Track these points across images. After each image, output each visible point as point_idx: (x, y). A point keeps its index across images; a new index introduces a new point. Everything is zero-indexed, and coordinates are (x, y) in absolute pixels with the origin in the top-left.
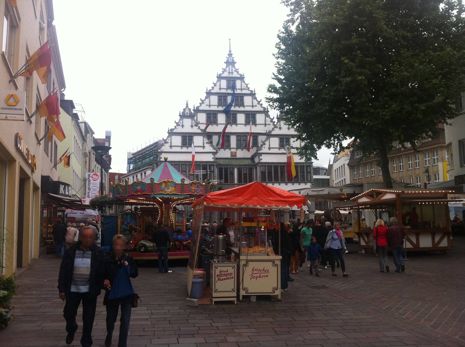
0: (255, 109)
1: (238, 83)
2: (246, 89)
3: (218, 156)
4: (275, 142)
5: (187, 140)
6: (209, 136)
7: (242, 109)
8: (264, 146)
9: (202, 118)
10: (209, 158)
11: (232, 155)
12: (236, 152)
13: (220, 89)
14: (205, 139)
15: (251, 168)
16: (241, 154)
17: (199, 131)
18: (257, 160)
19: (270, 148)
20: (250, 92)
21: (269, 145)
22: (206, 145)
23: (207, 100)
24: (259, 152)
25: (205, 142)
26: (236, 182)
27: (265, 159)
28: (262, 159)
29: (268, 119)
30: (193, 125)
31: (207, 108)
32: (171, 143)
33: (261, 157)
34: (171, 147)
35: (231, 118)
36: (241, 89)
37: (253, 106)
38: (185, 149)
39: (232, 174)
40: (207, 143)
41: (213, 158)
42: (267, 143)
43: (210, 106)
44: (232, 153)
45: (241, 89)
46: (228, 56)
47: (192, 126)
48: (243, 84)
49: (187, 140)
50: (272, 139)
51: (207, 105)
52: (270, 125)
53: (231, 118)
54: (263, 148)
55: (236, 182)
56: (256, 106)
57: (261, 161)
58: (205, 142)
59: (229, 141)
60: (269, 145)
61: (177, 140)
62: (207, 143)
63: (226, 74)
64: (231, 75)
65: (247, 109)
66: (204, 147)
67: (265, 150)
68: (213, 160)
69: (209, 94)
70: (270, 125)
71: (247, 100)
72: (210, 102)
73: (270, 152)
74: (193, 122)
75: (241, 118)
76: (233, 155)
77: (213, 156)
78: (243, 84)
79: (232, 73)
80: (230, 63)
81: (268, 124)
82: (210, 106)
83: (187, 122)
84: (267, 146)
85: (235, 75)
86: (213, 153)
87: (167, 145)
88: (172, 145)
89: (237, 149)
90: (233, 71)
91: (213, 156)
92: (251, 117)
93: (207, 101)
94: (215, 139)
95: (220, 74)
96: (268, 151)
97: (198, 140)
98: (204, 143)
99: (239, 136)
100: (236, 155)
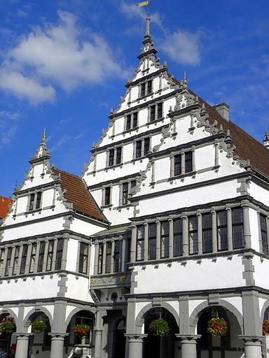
2: (168, 88)
4: (164, 166)
8: (143, 182)
14: (57, 192)
19: (152, 184)
21: (153, 176)
24: (134, 196)
25: (57, 197)
26: (123, 271)
31: (110, 142)
42: (149, 174)
60: (153, 176)
62: (58, 199)
64: (146, 74)
67: (144, 189)
72: (114, 130)
77: (64, 222)
79: (148, 69)
84: (148, 181)
90: (150, 67)
98: (54, 200)
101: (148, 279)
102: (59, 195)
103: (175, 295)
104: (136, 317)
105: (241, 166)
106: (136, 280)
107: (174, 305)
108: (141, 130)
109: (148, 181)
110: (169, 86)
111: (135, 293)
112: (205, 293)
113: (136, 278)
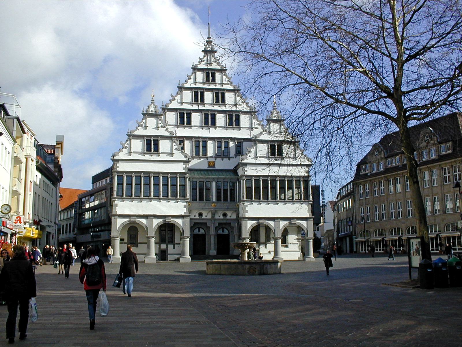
0: (239, 108)
1: (218, 75)
2: (228, 84)
3: (191, 165)
4: (263, 149)
5: (152, 145)
6: (181, 140)
7: (222, 108)
8: (249, 154)
9: (171, 118)
10: (180, 168)
11: (209, 166)
12: (214, 163)
13: (195, 83)
14: (174, 144)
15: (233, 183)
16: (220, 164)
17: (168, 134)
18: (240, 172)
19: (256, 157)
20: (232, 88)
22: (174, 151)
23: (178, 98)
24: (243, 162)
27: (250, 171)
28: (247, 171)
29: (254, 121)
30: (160, 125)
32: (130, 148)
33: (246, 169)
34: (130, 153)
35: (209, 119)
36: (222, 84)
37: (236, 105)
38: (147, 157)
39: (209, 190)
40: (176, 149)
41: (184, 169)
43: (181, 103)
44: (209, 163)
45: (222, 84)
46: (206, 44)
47: (157, 128)
48: (224, 77)
49: (152, 145)
50: (260, 145)
51: (178, 102)
52: (257, 128)
53: (209, 119)
54: (248, 157)
55: (214, 199)
56: (240, 105)
57: (246, 173)
58: (174, 147)
59: (205, 147)
61: (138, 145)
62: (176, 149)
63: (202, 66)
65: (228, 108)
66: (171, 154)
68: (184, 171)
69: (181, 88)
70: (257, 128)
71: (230, 97)
73: (257, 162)
74: (160, 122)
75: (221, 119)
76: (211, 165)
77: (184, 166)
78: (224, 77)
79: (211, 64)
80: (209, 52)
81: (256, 128)
82: (181, 103)
83: (151, 122)
84: (252, 155)
85: (215, 66)
86: (184, 162)
87: (125, 151)
88: (132, 151)
89: (216, 158)
91: (184, 166)
92: (233, 119)
93: (178, 98)
94: (187, 144)
95: (197, 65)
96: (253, 161)
97: (164, 146)
99: (218, 140)
100: (214, 166)
101: (255, 210)
102: (176, 147)
103: (273, 219)
104: (248, 228)
105: (308, 160)
106: (246, 209)
107: (271, 223)
108: (208, 107)
109: (252, 155)
110: (229, 83)
111: (247, 216)
112: (289, 219)
113: (247, 208)
